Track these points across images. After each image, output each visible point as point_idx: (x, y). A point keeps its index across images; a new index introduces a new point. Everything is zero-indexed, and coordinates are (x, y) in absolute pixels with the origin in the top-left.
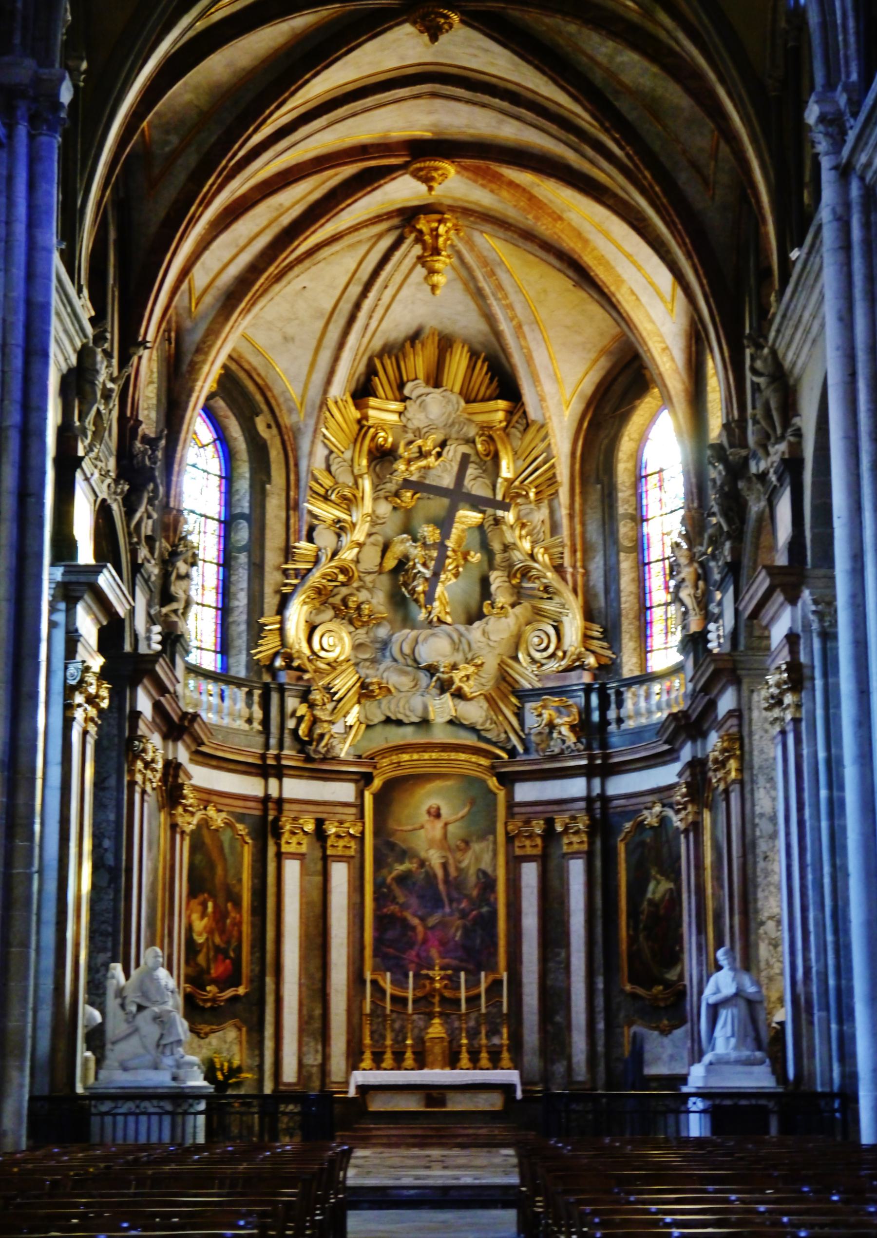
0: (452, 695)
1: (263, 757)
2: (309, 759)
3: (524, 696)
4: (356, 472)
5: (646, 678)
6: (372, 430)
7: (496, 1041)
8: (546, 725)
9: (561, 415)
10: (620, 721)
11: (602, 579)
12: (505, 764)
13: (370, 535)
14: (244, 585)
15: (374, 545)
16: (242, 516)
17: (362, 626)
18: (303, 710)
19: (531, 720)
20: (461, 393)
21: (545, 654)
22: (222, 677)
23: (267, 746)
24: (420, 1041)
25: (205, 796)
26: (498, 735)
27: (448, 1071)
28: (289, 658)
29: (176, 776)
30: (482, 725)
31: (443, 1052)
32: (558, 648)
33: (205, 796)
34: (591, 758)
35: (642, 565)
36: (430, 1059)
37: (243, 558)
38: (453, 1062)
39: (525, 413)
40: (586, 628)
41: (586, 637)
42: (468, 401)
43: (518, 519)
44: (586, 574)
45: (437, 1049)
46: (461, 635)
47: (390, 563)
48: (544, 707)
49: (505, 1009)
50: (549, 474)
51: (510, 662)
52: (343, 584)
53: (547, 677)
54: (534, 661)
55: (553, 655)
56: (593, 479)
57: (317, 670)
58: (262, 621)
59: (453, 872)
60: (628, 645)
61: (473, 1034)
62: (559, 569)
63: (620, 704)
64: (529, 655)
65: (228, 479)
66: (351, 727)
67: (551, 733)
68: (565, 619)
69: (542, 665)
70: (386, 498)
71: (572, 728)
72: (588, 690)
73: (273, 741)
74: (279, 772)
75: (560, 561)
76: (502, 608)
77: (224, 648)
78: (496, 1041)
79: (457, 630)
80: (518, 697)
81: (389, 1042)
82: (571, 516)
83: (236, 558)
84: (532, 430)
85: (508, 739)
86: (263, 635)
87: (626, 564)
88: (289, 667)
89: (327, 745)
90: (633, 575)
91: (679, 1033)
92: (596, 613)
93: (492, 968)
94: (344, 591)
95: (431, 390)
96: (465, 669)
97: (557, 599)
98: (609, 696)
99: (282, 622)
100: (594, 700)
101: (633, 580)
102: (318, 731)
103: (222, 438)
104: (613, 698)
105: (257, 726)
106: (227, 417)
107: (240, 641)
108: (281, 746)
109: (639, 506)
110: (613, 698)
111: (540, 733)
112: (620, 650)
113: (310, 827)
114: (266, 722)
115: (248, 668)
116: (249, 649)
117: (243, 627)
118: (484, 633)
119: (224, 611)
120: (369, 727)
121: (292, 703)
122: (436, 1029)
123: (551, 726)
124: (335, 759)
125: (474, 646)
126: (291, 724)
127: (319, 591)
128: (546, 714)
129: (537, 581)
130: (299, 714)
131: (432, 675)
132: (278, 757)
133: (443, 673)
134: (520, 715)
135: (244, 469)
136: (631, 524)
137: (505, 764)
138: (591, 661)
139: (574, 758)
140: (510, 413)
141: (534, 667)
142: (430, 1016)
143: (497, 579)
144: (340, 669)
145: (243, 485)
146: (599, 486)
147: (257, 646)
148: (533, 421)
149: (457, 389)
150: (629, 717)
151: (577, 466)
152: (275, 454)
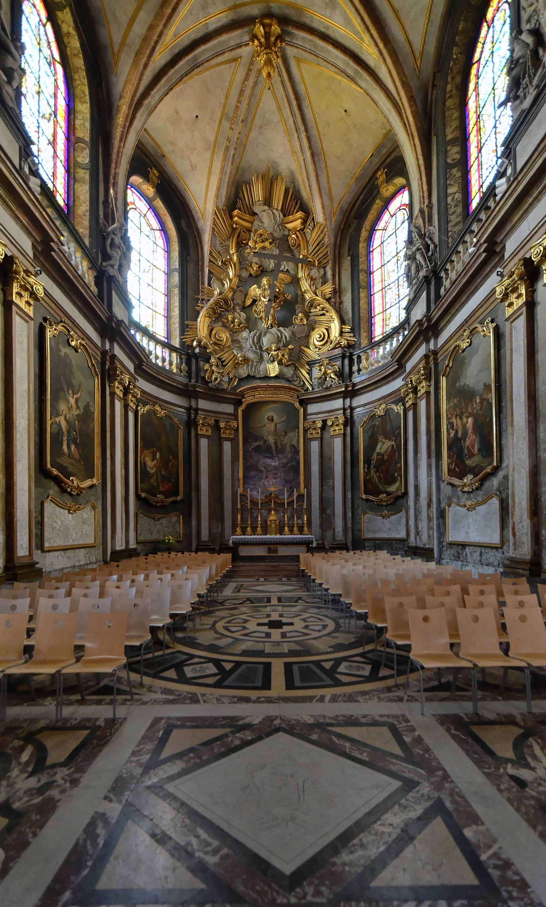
0: (278, 364)
1: (186, 385)
2: (210, 389)
3: (311, 364)
4: (231, 252)
5: (374, 345)
6: (238, 231)
7: (300, 522)
8: (324, 374)
9: (331, 221)
10: (359, 370)
11: (350, 304)
12: (303, 395)
13: (238, 287)
14: (177, 304)
15: (241, 291)
16: (175, 270)
17: (236, 332)
18: (207, 367)
19: (317, 373)
20: (282, 210)
21: (323, 342)
22: (166, 345)
23: (190, 381)
24: (265, 522)
25: (155, 400)
26: (299, 383)
27: (278, 536)
28: (199, 342)
29: (112, 363)
30: (292, 378)
31: (276, 527)
32: (329, 337)
33: (155, 400)
34: (347, 387)
35: (370, 295)
36: (269, 530)
37: (176, 291)
38: (281, 532)
39: (313, 219)
40: (342, 328)
41: (341, 333)
42: (285, 216)
43: (308, 275)
44: (341, 303)
45: (273, 525)
46: (281, 333)
47: (249, 302)
48: (322, 365)
49: (305, 507)
50: (325, 252)
51: (306, 349)
52: (227, 310)
53: (323, 354)
54: (316, 347)
55: (327, 342)
56: (346, 253)
57: (214, 350)
58: (186, 322)
59: (279, 446)
60: (364, 335)
61: (291, 518)
62: (328, 300)
63: (359, 362)
64: (314, 345)
65: (168, 251)
66: (231, 379)
67: (326, 378)
68: (332, 325)
69: (320, 349)
70: (247, 270)
71: (335, 375)
72: (343, 357)
73: (193, 381)
74: (196, 396)
75: (330, 296)
76: (301, 320)
77: (168, 336)
78: (300, 522)
79: (280, 331)
80: (308, 364)
81: (249, 522)
82: (334, 276)
83: (173, 291)
84: (316, 230)
85: (304, 383)
86: (188, 329)
87: (363, 294)
88: (199, 345)
89: (219, 383)
90: (367, 300)
91: (394, 518)
92: (346, 322)
93: (298, 488)
94: (227, 313)
95: (266, 208)
96: (284, 350)
97: (328, 314)
98: (354, 359)
99: (196, 325)
100: (346, 361)
101: (366, 302)
102: (214, 377)
103: (163, 229)
104: (356, 360)
105: (184, 373)
106: (165, 215)
107: (176, 332)
108: (197, 382)
109: (369, 266)
110: (356, 360)
111: (321, 378)
112: (360, 336)
113: (212, 422)
114: (189, 372)
115: (180, 345)
116: (180, 336)
117: (177, 325)
118: (293, 333)
119: (168, 318)
120: (239, 379)
121: (202, 363)
122: (273, 517)
123: (325, 373)
124: (223, 390)
125: (288, 338)
126: (202, 374)
127: (214, 309)
128: (323, 370)
129: (318, 307)
130: (205, 368)
131: (269, 354)
132: (194, 386)
133: (275, 351)
134: (310, 373)
135: (176, 247)
136: (365, 275)
137: (303, 395)
138: (344, 343)
139: (337, 387)
140: (304, 222)
141: (317, 350)
142: (270, 510)
143: (298, 308)
144: (226, 350)
145: (176, 254)
146: (349, 258)
147: (184, 335)
148: (318, 223)
149: (280, 208)
150: (365, 368)
151: (337, 250)
152: (191, 242)
